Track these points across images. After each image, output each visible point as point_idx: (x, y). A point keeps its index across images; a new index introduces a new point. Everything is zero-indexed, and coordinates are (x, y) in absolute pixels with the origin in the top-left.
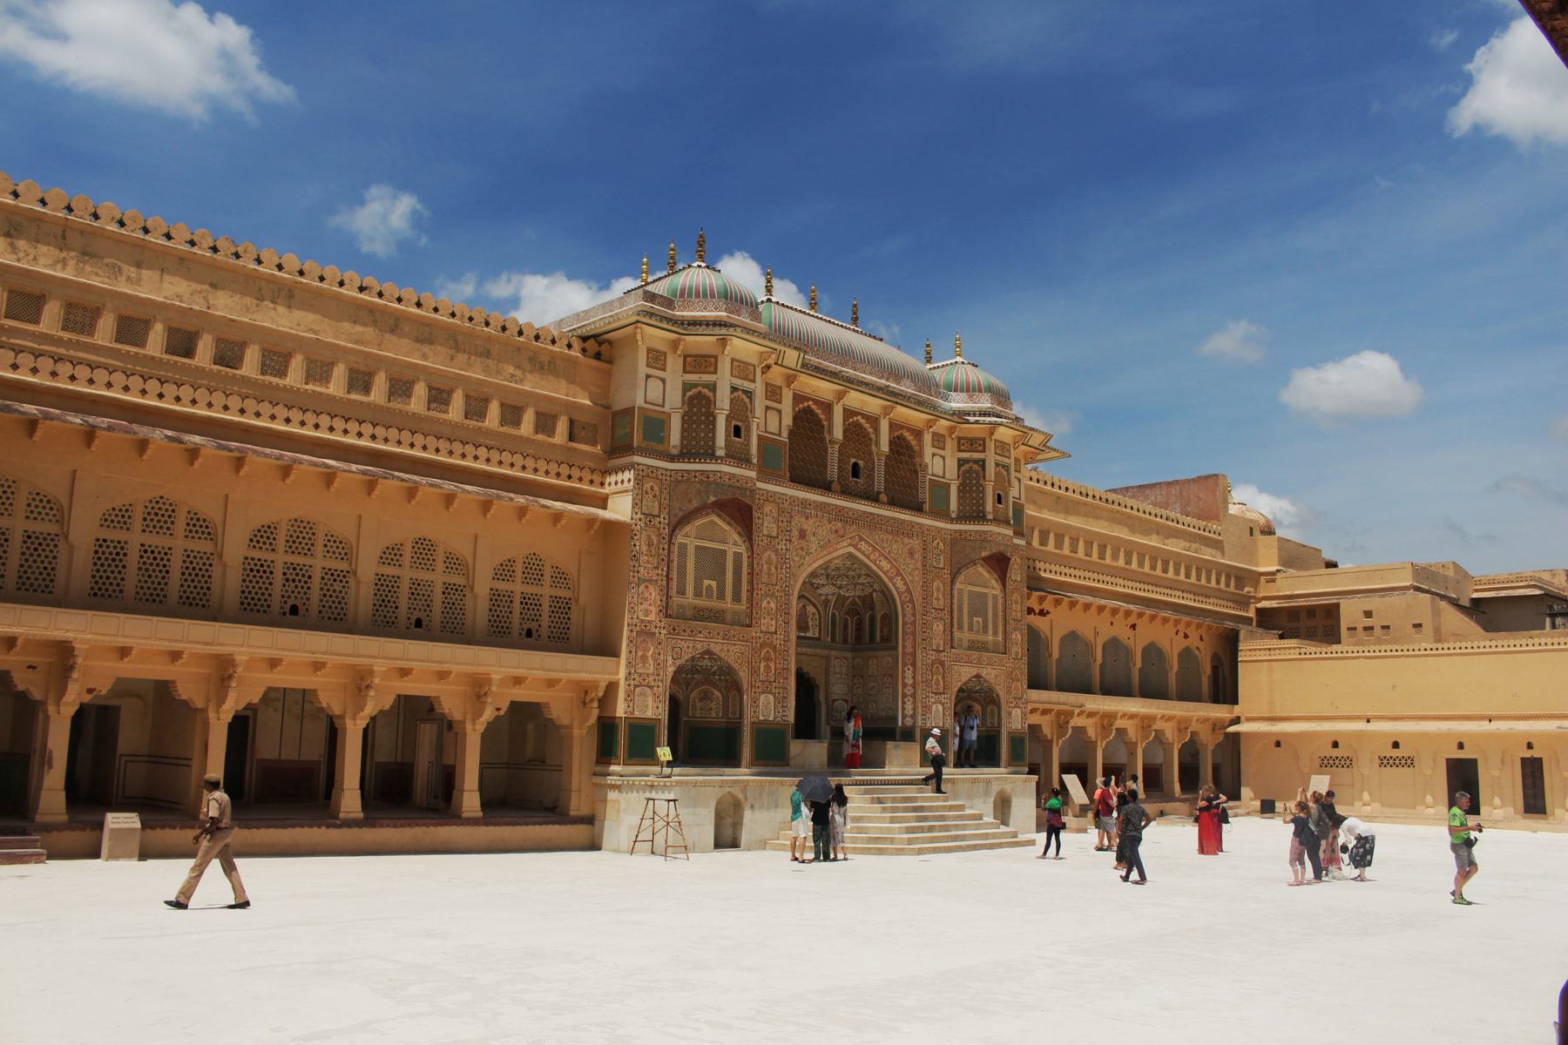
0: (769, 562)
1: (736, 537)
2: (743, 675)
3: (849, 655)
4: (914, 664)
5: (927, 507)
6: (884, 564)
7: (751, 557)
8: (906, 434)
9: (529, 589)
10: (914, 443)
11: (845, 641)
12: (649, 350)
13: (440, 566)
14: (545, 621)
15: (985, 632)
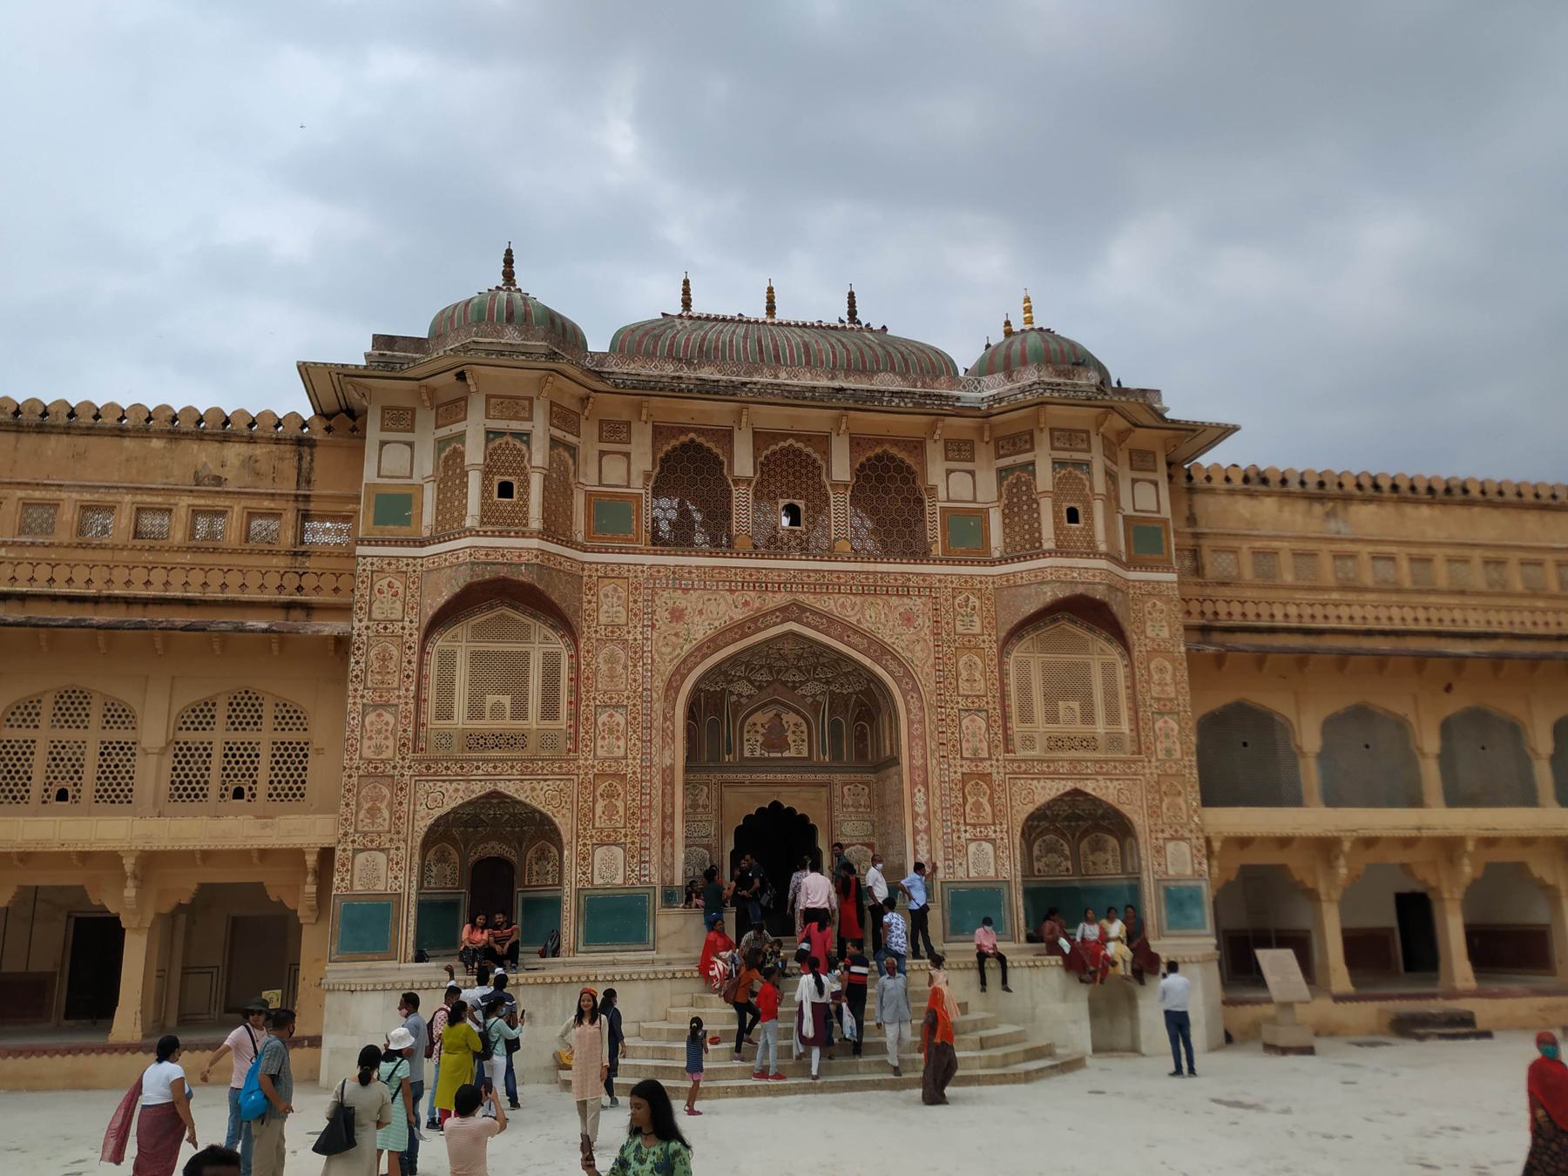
0: (612, 660)
1: (550, 633)
2: (564, 823)
3: (872, 777)
4: (926, 784)
5: (937, 550)
6: (855, 639)
7: (575, 657)
8: (894, 451)
9: (239, 736)
10: (909, 461)
11: (861, 755)
12: (384, 409)
13: (96, 720)
14: (264, 774)
15: (1088, 717)
